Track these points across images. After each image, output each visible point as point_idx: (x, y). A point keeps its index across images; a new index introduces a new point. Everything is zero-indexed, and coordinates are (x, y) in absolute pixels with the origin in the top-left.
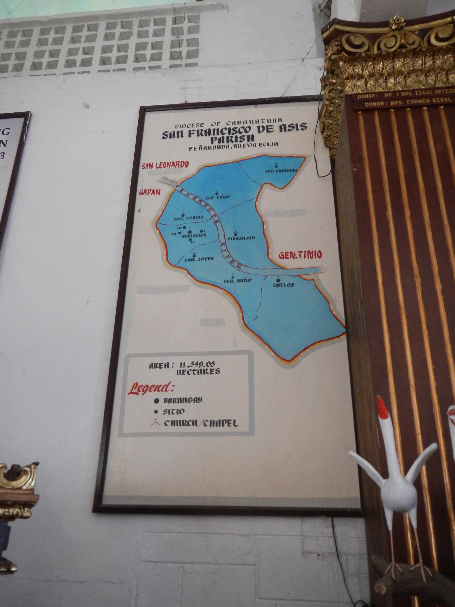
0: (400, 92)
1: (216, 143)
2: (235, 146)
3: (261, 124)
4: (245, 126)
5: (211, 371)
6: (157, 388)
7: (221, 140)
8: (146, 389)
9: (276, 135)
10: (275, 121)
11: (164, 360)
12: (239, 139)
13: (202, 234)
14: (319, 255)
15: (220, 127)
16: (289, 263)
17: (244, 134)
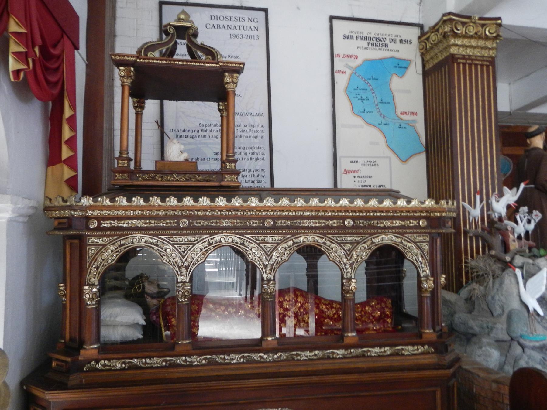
0: (471, 56)
1: (370, 45)
2: (379, 49)
3: (391, 38)
4: (384, 37)
5: (375, 165)
6: (354, 171)
8: (350, 172)
9: (398, 46)
10: (397, 36)
11: (356, 160)
13: (367, 99)
14: (416, 114)
15: (372, 36)
16: (404, 117)
17: (383, 42)
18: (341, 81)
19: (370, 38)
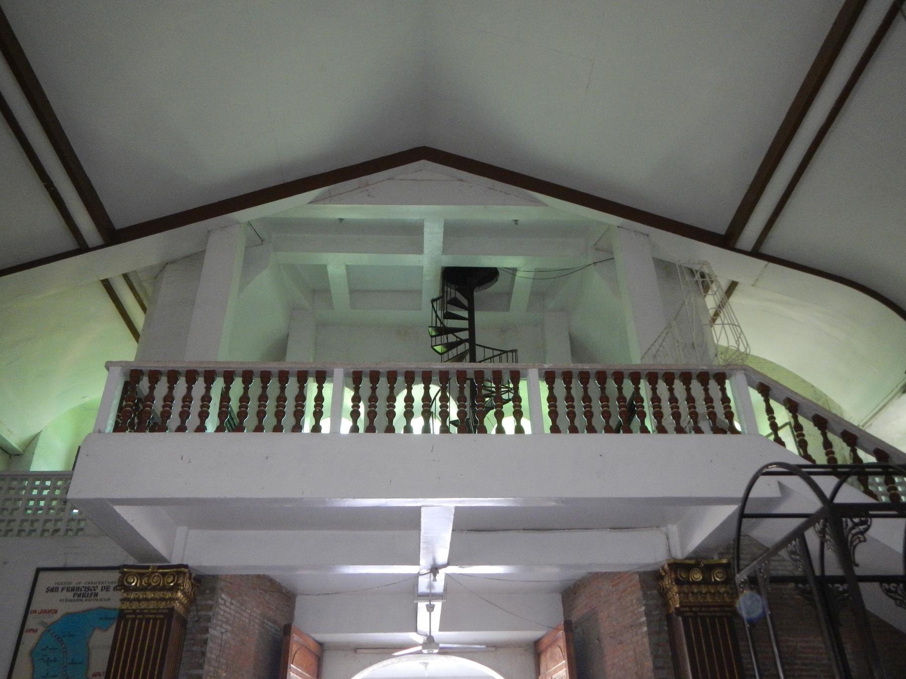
1: (76, 597)
2: (86, 600)
3: (104, 585)
4: (95, 586)
7: (79, 596)
12: (89, 595)
13: (55, 660)
15: (81, 585)
17: (93, 591)
18: (29, 640)
19: (78, 589)
